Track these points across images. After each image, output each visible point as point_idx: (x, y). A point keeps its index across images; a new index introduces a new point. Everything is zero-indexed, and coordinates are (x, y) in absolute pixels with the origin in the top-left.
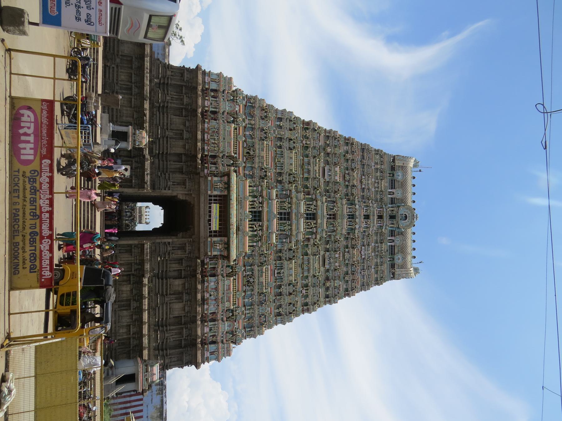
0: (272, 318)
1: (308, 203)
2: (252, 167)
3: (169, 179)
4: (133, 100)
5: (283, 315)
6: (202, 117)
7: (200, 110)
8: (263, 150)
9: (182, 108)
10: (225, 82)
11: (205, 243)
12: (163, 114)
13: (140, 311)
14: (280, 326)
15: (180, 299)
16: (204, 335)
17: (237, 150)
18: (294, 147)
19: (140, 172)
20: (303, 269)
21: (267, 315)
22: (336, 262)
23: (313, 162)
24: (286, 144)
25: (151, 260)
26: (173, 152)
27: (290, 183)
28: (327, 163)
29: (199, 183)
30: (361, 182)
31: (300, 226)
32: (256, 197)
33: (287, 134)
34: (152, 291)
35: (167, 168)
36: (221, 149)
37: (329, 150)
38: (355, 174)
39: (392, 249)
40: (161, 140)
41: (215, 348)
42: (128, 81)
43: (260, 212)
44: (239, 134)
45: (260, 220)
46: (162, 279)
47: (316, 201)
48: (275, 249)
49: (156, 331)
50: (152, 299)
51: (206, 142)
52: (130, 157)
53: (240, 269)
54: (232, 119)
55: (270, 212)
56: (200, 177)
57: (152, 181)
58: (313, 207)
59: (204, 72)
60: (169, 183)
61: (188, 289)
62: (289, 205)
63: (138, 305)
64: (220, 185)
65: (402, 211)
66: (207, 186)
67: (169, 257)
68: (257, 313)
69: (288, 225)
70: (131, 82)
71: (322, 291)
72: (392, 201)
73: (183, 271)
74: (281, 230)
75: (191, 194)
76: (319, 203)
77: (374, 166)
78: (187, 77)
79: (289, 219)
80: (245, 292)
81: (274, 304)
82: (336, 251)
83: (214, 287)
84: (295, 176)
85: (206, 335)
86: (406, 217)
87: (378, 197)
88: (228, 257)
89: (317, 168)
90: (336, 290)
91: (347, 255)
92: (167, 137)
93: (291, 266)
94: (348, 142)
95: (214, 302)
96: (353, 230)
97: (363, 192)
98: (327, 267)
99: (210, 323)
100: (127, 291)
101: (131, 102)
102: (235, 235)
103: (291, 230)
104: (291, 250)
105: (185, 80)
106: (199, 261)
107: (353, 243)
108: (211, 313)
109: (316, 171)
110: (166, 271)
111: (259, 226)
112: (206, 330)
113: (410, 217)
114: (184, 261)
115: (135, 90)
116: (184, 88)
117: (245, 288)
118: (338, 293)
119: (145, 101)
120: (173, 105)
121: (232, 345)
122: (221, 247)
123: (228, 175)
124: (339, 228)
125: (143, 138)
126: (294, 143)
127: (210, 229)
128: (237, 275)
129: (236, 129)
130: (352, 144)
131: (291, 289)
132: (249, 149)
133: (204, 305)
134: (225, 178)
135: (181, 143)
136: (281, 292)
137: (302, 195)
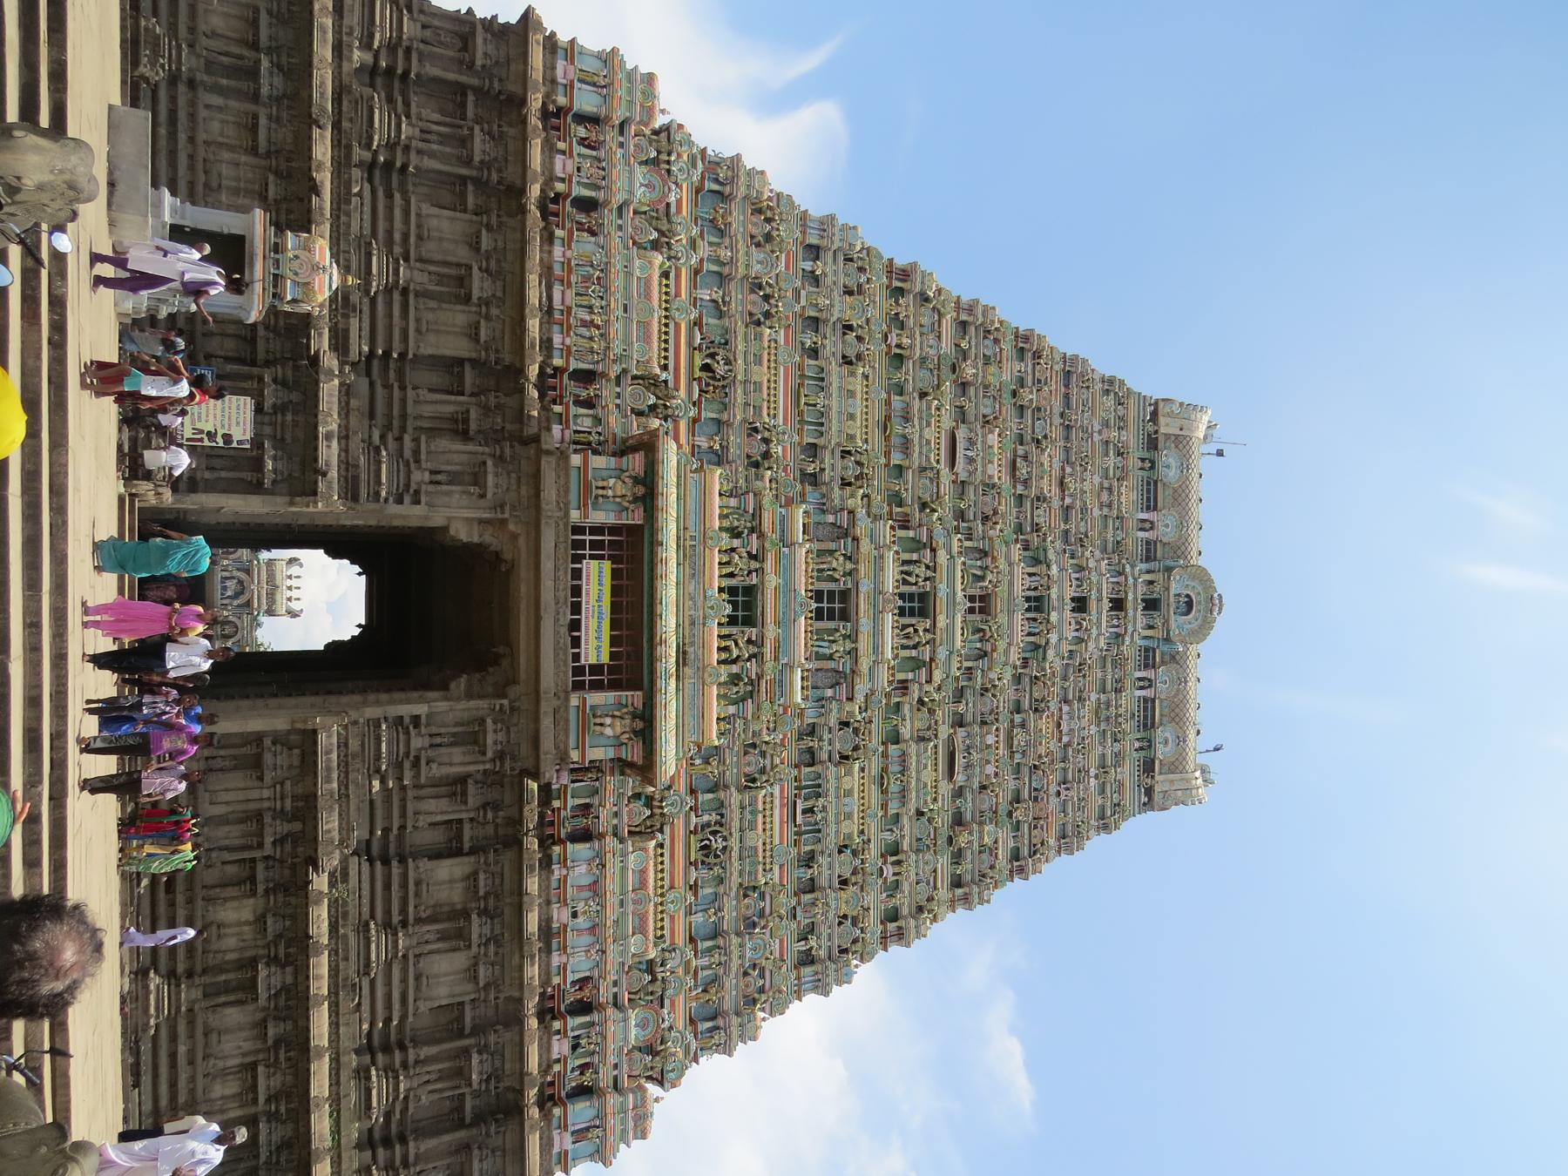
0: (785, 977)
1: (906, 556)
2: (719, 422)
3: (417, 461)
4: (263, 121)
5: (823, 961)
6: (544, 217)
7: (535, 191)
8: (758, 361)
9: (463, 180)
10: (630, 91)
11: (559, 714)
12: (389, 195)
13: (295, 1002)
14: (811, 999)
15: (457, 937)
16: (549, 1067)
17: (671, 354)
18: (859, 357)
19: (295, 424)
20: (884, 792)
21: (769, 965)
22: (988, 762)
23: (920, 410)
24: (832, 345)
25: (344, 796)
26: (430, 351)
27: (845, 484)
28: (961, 415)
29: (536, 477)
30: (1062, 483)
31: (880, 636)
32: (738, 535)
33: (841, 308)
34: (345, 914)
35: (404, 416)
36: (617, 348)
37: (969, 371)
38: (1045, 459)
39: (1145, 709)
40: (380, 299)
41: (592, 1113)
42: (242, 42)
43: (750, 591)
44: (678, 295)
45: (749, 621)
46: (386, 862)
47: (933, 550)
48: (798, 722)
49: (362, 1074)
50: (346, 950)
51: (557, 316)
52: (253, 363)
53: (677, 807)
54: (655, 235)
55: (788, 589)
56: (541, 452)
57: (346, 464)
58: (920, 571)
59: (551, 43)
60: (417, 476)
61: (487, 894)
62: (849, 566)
63: (289, 980)
64: (617, 487)
65: (1177, 586)
66: (567, 491)
67: (417, 776)
68: (735, 963)
69: (845, 637)
70: (254, 46)
71: (943, 862)
72: (1150, 552)
73: (467, 827)
74: (819, 657)
75: (503, 522)
76: (942, 557)
77: (1100, 432)
78: (485, 54)
79: (845, 616)
80: (694, 888)
81: (794, 926)
82: (984, 723)
83: (586, 881)
84: (864, 459)
85: (556, 1068)
86: (1189, 604)
87: (1110, 537)
88: (646, 768)
89: (929, 434)
90: (985, 856)
91: (1020, 737)
92: (405, 292)
93: (847, 783)
94: (1027, 346)
95: (586, 939)
96: (1037, 649)
97: (1066, 521)
98: (960, 778)
99: (573, 1022)
100: (239, 924)
101: (254, 129)
102: (673, 682)
103: (853, 653)
104: (847, 724)
105: (479, 62)
106: (534, 786)
107: (1036, 695)
108: (574, 983)
109: (928, 442)
110: (403, 827)
111: (749, 641)
112: (560, 1047)
113: (1201, 605)
114: (471, 789)
115: (270, 82)
116: (471, 98)
117: (694, 874)
118: (992, 867)
119: (316, 132)
120: (428, 163)
121: (653, 1089)
122: (618, 730)
123: (648, 446)
124: (1001, 645)
125: (316, 268)
126: (859, 339)
127: (576, 657)
128: (667, 829)
129: (666, 275)
130: (1037, 355)
131: (843, 865)
132: (712, 356)
133: (549, 952)
134: (636, 462)
135: (459, 317)
136: (812, 880)
137: (885, 530)
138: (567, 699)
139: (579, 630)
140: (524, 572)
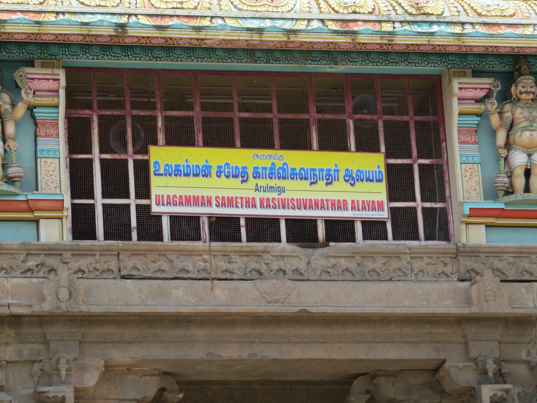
127: (374, 229)
138: (474, 252)
139: (312, 222)
140: (195, 352)
